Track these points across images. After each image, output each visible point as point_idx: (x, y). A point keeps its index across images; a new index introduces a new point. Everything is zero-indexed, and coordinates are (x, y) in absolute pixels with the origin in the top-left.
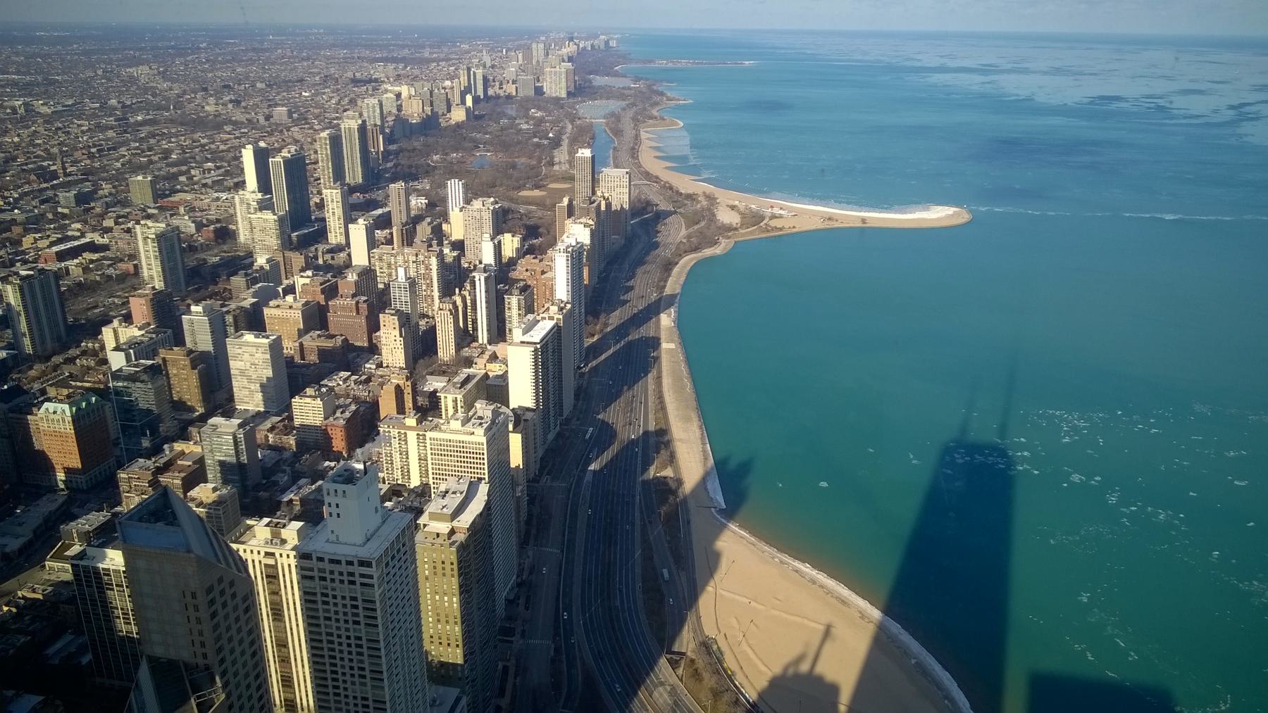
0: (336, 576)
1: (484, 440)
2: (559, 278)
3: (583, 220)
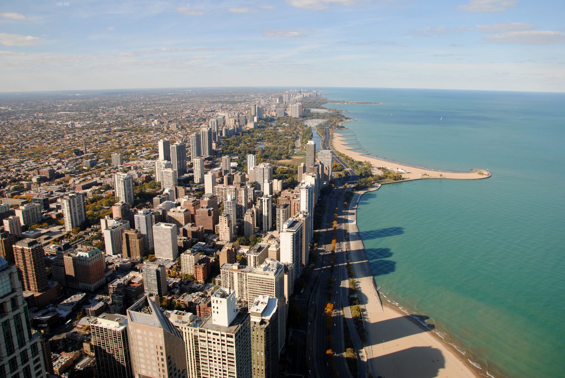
0: (216, 341)
1: (274, 278)
2: (303, 201)
3: (311, 174)
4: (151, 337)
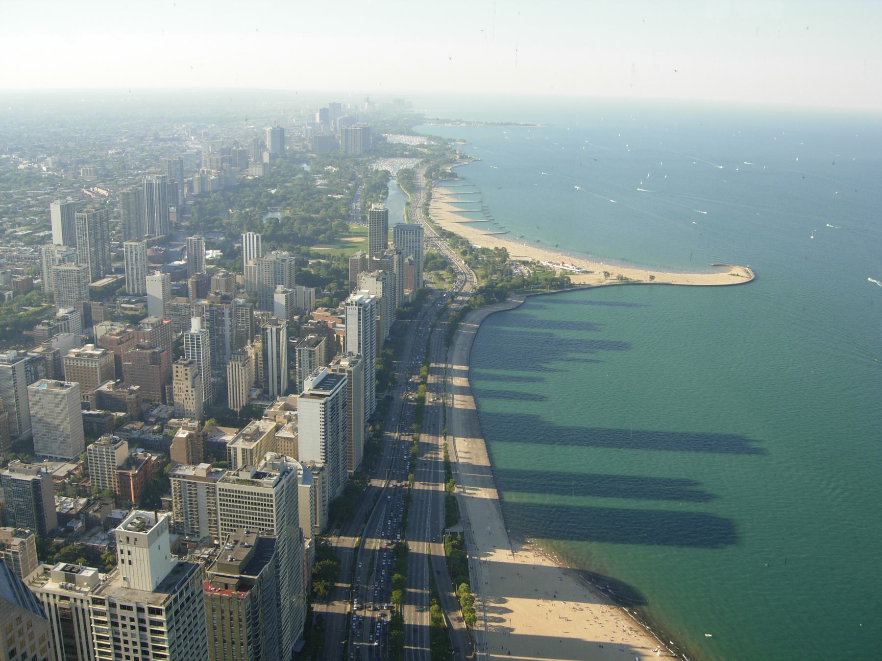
0: (127, 622)
3: (375, 273)
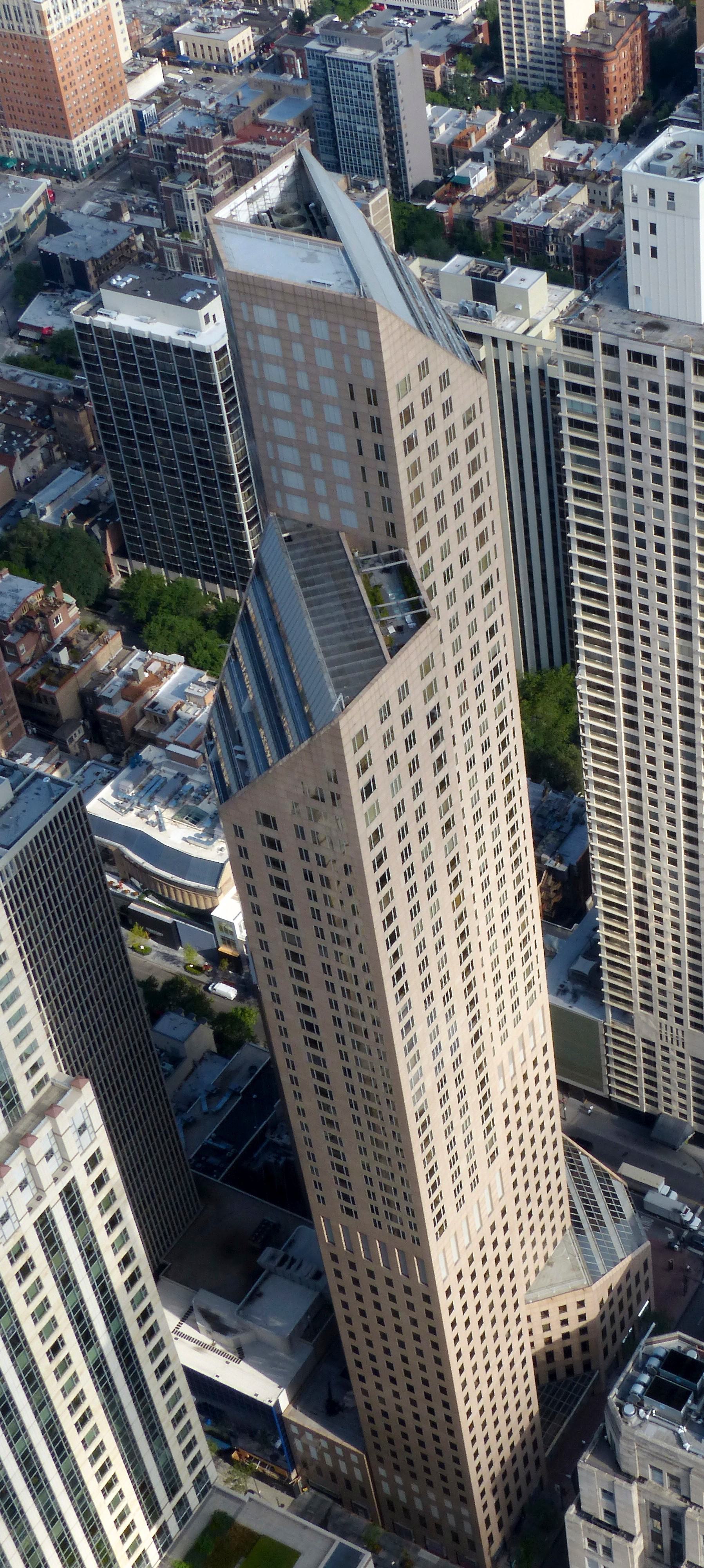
4: (324, 345)
